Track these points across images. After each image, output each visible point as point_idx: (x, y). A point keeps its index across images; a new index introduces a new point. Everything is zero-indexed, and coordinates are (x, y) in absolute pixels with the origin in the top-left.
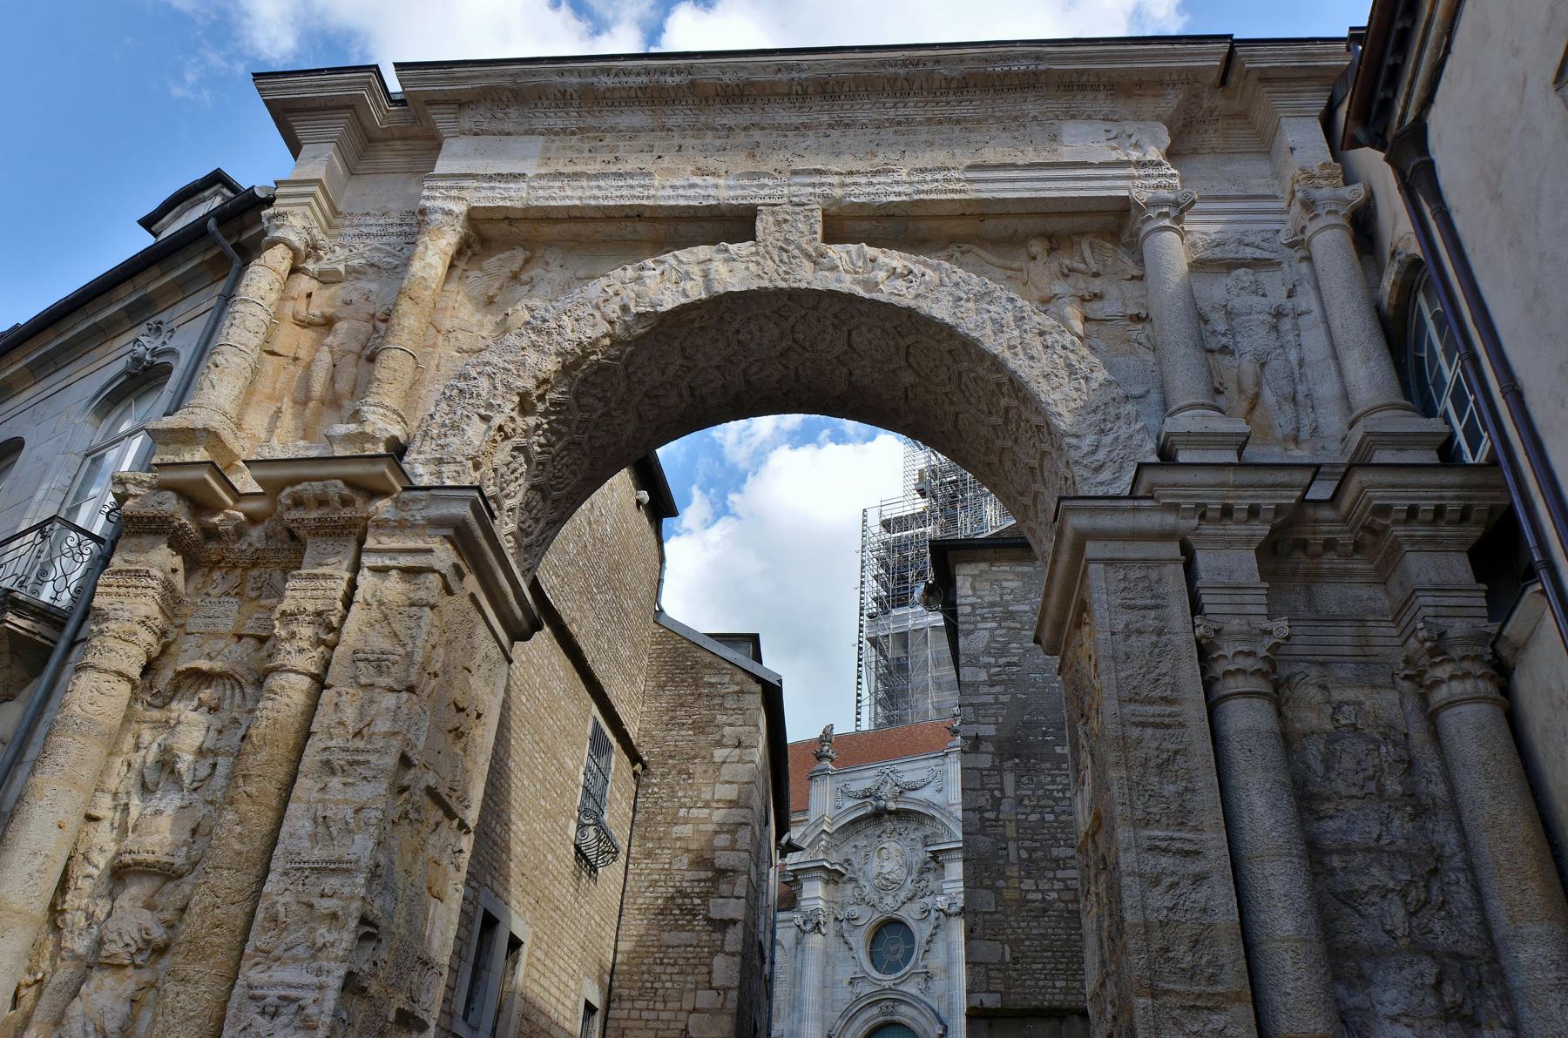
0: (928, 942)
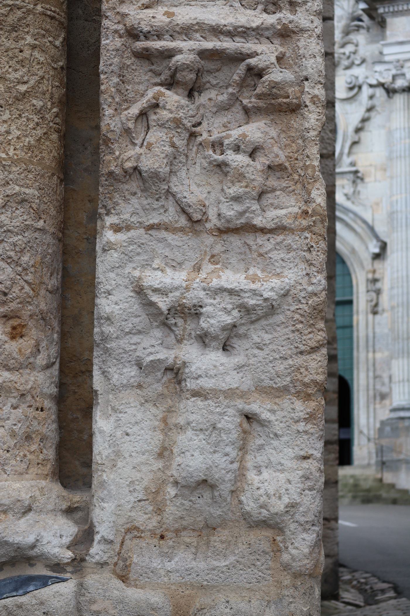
0: (358, 130)
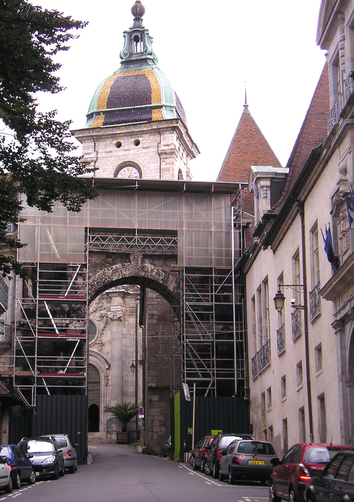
0: (103, 330)
